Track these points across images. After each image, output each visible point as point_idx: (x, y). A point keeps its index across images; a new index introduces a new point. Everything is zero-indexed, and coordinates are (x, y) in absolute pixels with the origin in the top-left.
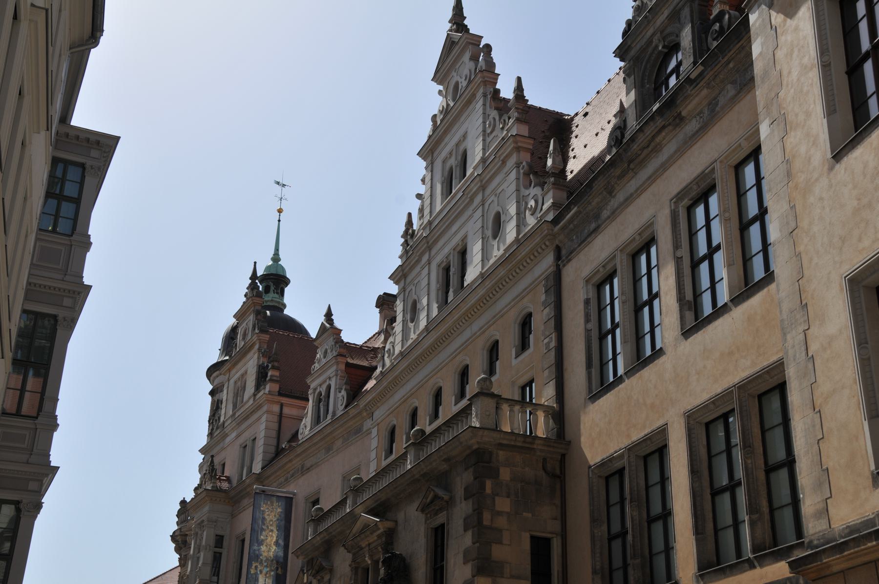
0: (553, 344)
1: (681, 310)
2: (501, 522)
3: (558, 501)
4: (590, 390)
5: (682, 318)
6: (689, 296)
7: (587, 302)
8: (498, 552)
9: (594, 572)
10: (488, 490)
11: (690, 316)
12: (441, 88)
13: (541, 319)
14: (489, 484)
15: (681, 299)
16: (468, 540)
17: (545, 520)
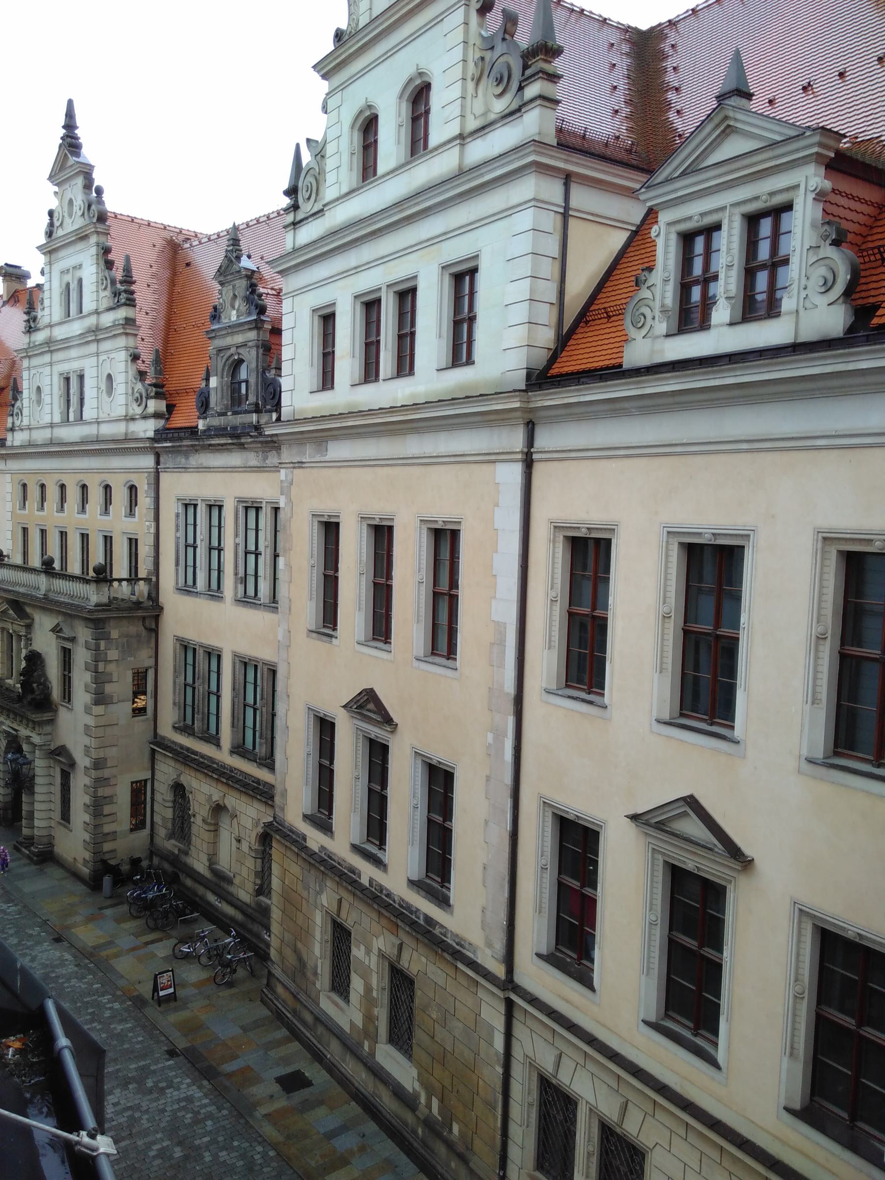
0: (152, 530)
1: (236, 582)
2: (111, 668)
3: (153, 645)
4: (177, 583)
5: (236, 588)
6: (241, 573)
7: (177, 515)
8: (109, 688)
9: (174, 704)
10: (102, 648)
11: (241, 588)
12: (56, 189)
13: (145, 500)
14: (103, 644)
15: (236, 574)
16: (88, 677)
17: (144, 658)
